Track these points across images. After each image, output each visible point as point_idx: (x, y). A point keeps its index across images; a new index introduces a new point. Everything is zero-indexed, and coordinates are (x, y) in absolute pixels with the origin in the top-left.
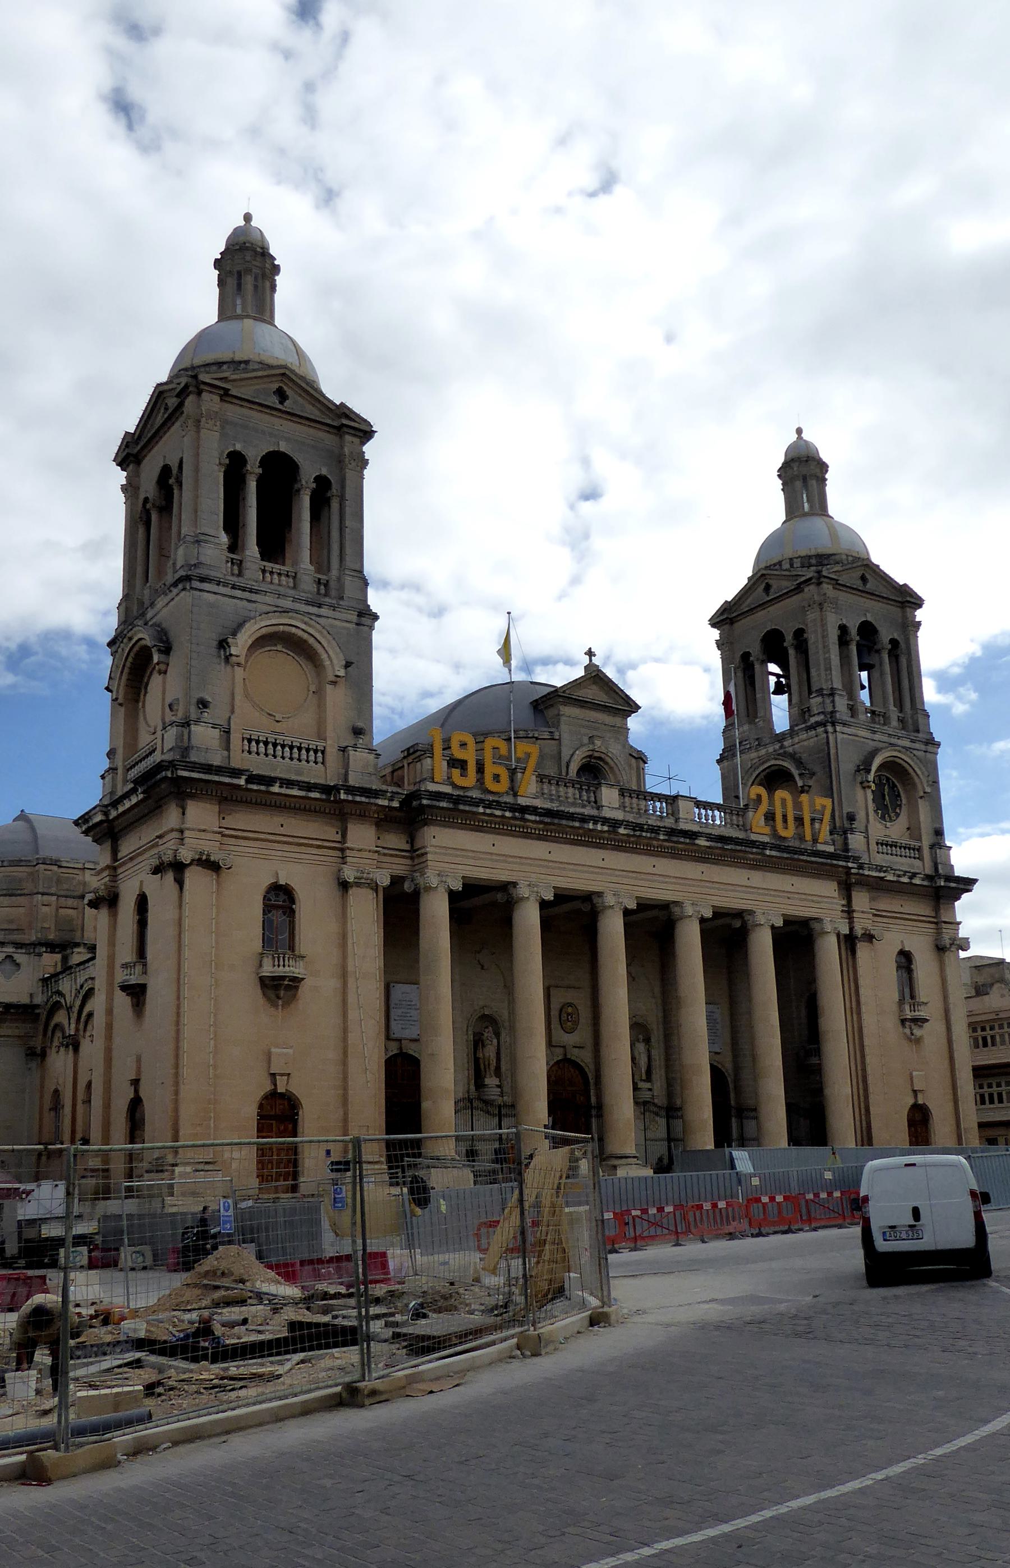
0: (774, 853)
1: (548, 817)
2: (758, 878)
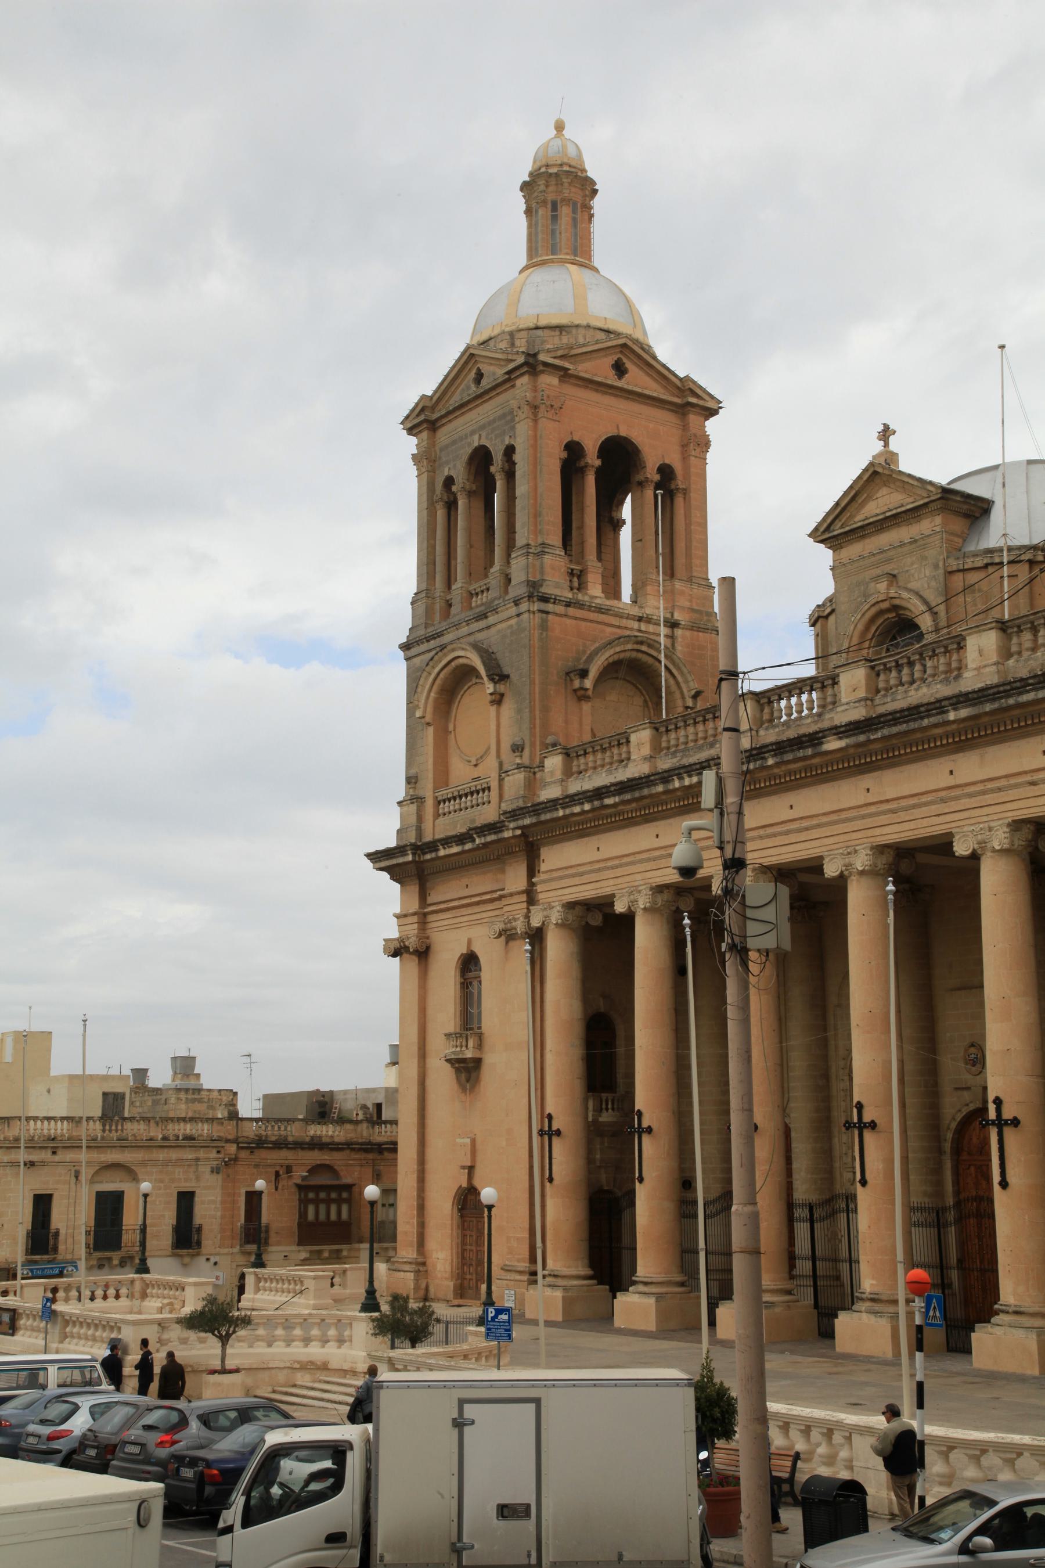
0: (964, 713)
1: (626, 792)
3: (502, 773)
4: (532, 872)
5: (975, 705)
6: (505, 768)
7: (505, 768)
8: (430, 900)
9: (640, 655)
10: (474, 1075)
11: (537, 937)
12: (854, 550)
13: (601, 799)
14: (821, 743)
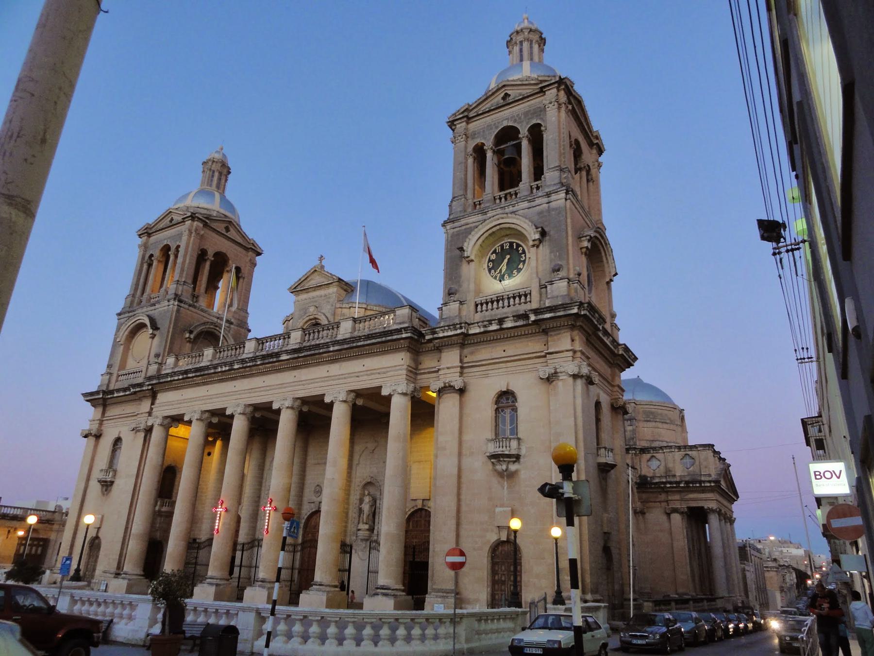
2: (335, 369)
3: (149, 364)
4: (153, 404)
5: (340, 345)
6: (150, 363)
7: (150, 363)
8: (106, 415)
9: (215, 331)
10: (109, 488)
11: (149, 431)
12: (304, 296)
13: (187, 374)
14: (280, 357)
